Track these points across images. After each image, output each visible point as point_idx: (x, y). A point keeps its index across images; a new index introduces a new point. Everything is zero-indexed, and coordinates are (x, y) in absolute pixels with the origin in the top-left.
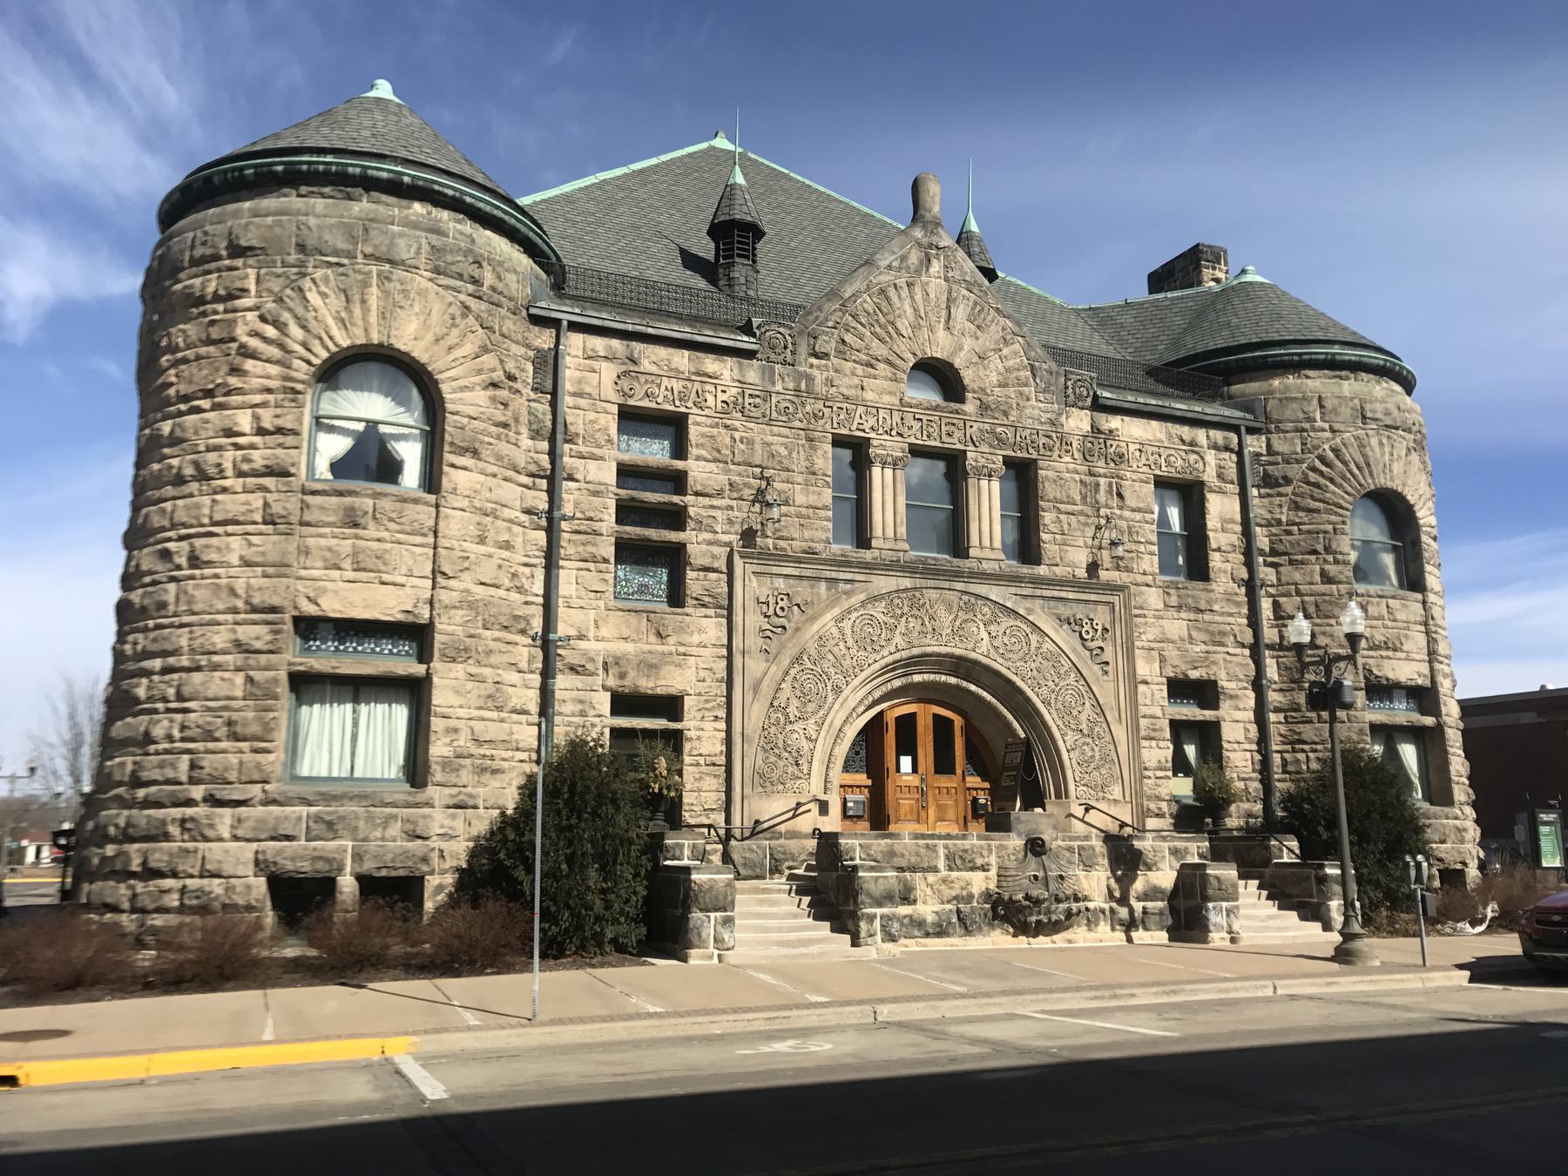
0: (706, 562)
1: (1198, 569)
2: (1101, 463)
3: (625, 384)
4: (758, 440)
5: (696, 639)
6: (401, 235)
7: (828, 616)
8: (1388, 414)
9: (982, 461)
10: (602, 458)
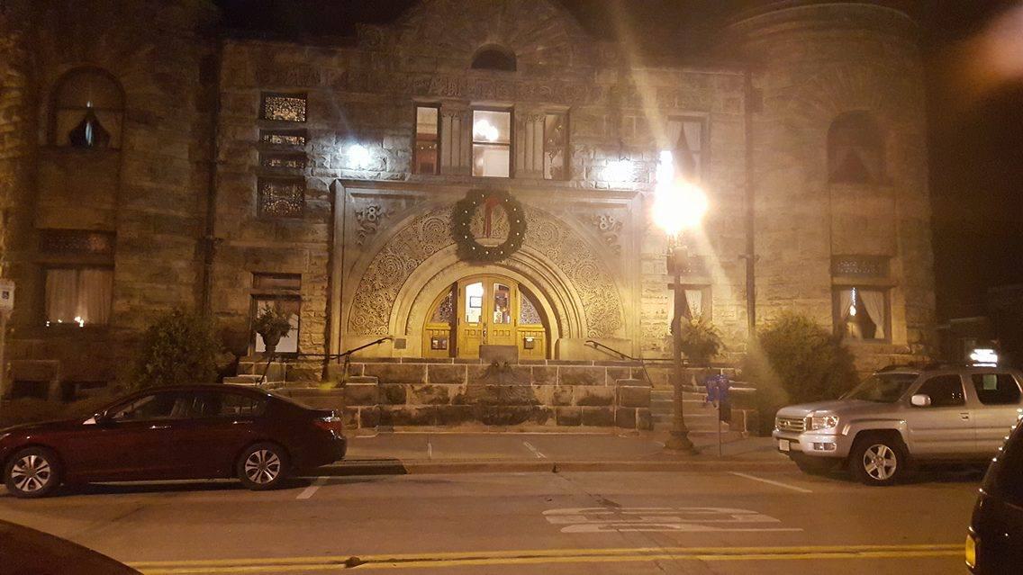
7: (406, 221)
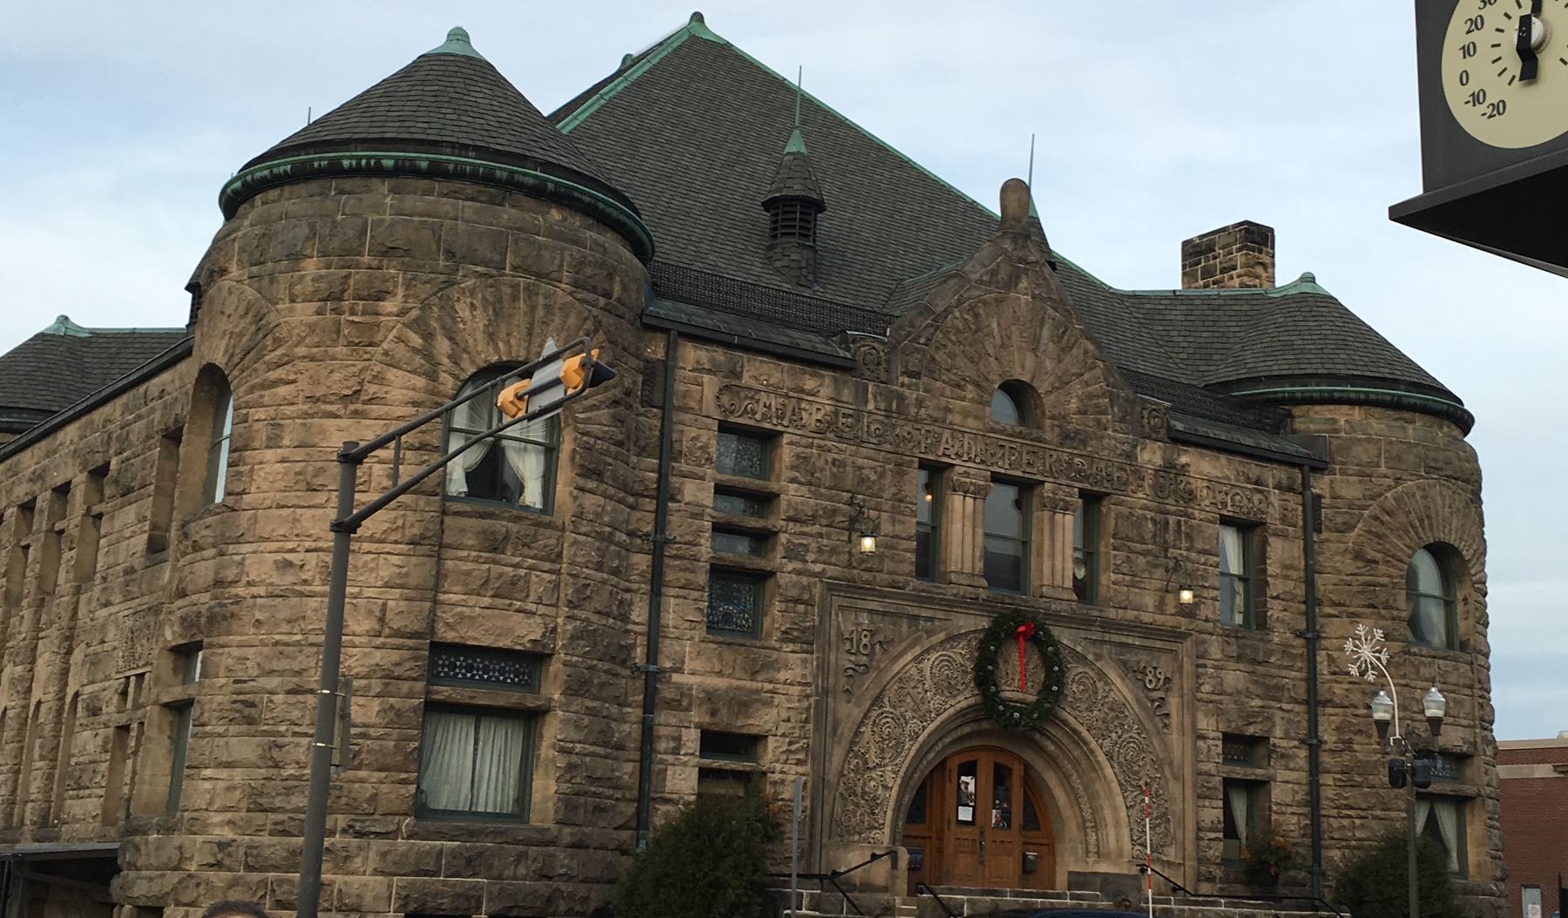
0: (794, 593)
1: (1257, 619)
2: (1171, 501)
3: (725, 400)
4: (849, 462)
5: (783, 675)
6: (546, 247)
7: (909, 657)
9: (1061, 495)
10: (702, 478)
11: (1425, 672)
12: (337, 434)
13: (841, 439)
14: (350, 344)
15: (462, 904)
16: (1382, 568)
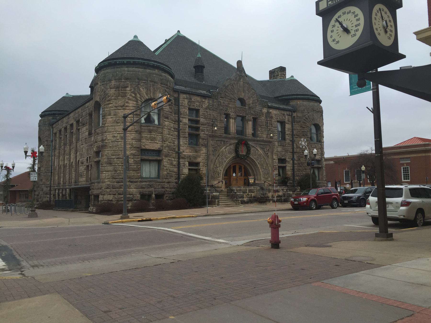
1: (284, 138)
3: (189, 104)
5: (202, 152)
8: (317, 109)
11: (313, 146)
12: (121, 113)
13: (210, 110)
14: (121, 96)
15: (150, 193)
16: (305, 129)
